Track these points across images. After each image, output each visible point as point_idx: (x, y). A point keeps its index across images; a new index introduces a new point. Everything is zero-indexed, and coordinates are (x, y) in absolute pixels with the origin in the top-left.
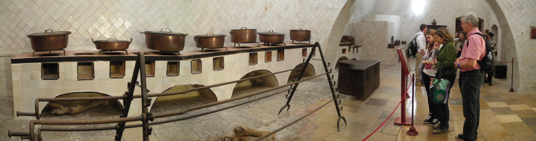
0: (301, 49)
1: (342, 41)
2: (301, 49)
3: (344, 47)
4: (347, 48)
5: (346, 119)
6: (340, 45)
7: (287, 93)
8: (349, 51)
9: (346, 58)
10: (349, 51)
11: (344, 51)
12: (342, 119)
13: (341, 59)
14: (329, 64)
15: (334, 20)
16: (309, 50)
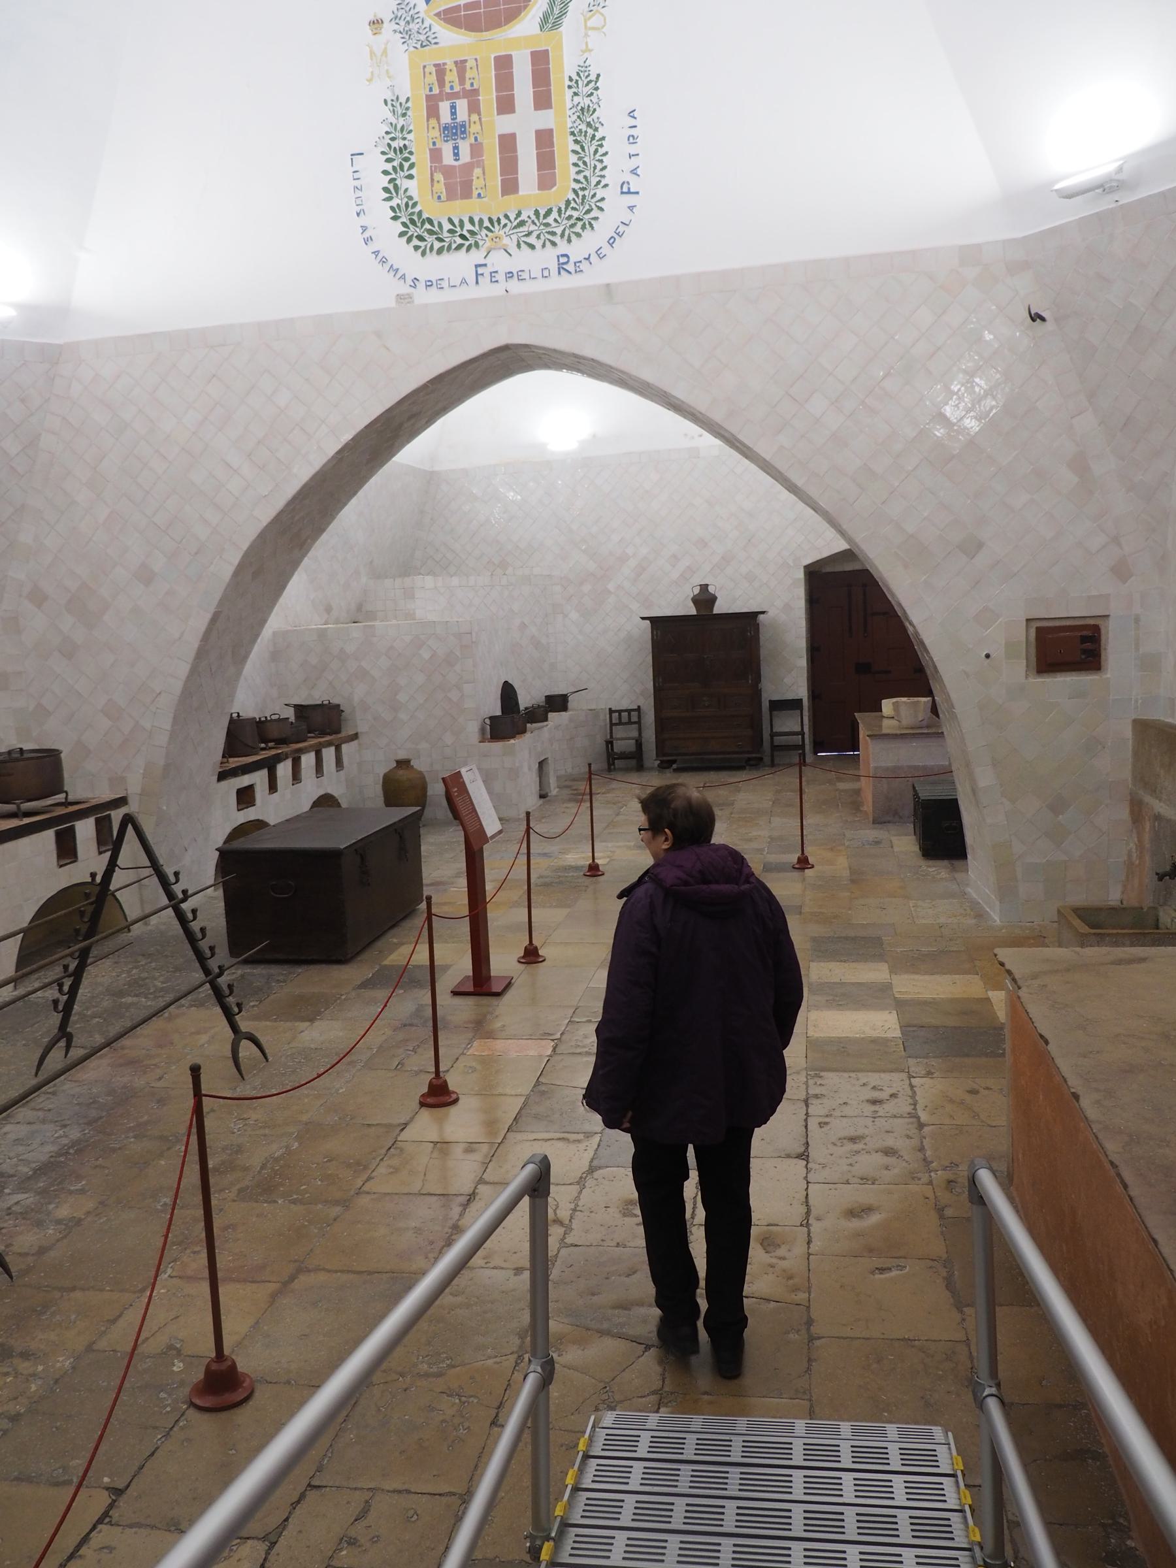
0: (49, 835)
1: (231, 749)
2: (49, 835)
3: (245, 780)
4: (259, 779)
5: (263, 1040)
6: (222, 776)
7: (52, 993)
8: (273, 787)
9: (259, 824)
10: (273, 787)
11: (245, 797)
12: (245, 1043)
13: (239, 832)
14: (176, 874)
15: (177, 686)
16: (85, 830)
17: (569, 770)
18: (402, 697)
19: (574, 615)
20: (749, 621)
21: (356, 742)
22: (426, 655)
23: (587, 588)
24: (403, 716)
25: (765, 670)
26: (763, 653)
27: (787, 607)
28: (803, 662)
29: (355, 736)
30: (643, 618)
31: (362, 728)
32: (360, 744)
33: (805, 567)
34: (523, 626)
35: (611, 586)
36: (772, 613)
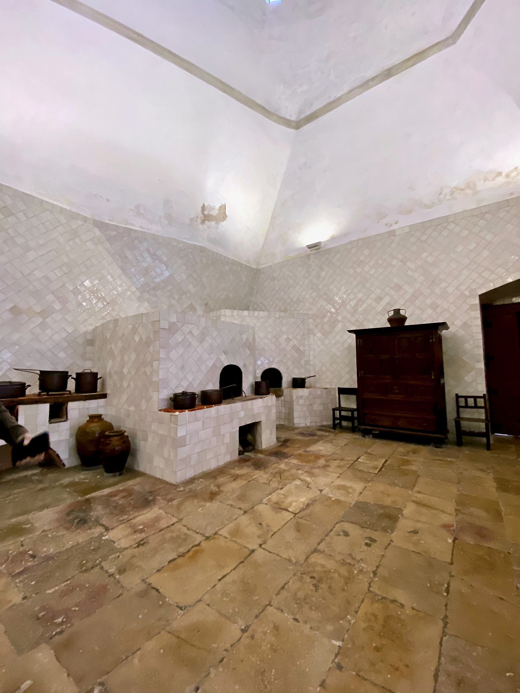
17: (308, 424)
18: (125, 371)
19: (319, 335)
20: (431, 334)
21: (102, 401)
22: (137, 339)
23: (326, 320)
24: (125, 385)
25: (447, 370)
26: (445, 358)
27: (465, 325)
28: (482, 365)
29: (104, 396)
30: (350, 331)
31: (108, 392)
32: (107, 402)
33: (480, 296)
34: (288, 340)
35: (339, 318)
36: (452, 329)
